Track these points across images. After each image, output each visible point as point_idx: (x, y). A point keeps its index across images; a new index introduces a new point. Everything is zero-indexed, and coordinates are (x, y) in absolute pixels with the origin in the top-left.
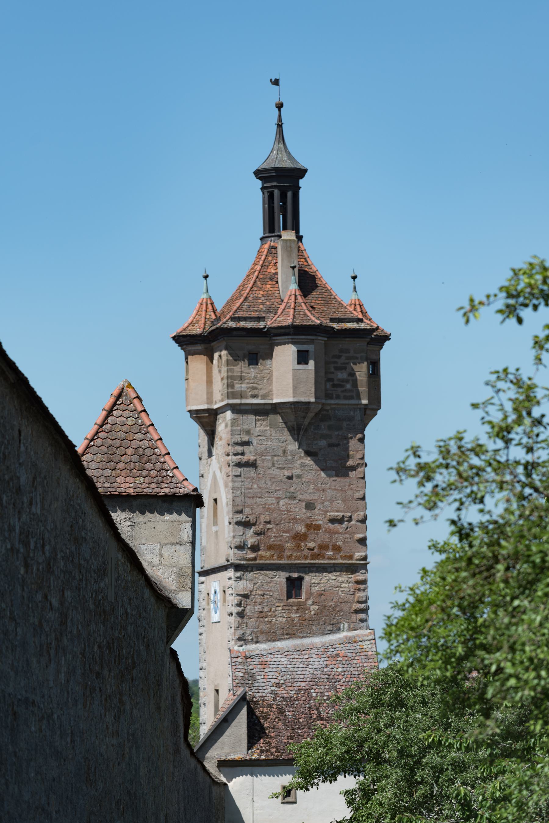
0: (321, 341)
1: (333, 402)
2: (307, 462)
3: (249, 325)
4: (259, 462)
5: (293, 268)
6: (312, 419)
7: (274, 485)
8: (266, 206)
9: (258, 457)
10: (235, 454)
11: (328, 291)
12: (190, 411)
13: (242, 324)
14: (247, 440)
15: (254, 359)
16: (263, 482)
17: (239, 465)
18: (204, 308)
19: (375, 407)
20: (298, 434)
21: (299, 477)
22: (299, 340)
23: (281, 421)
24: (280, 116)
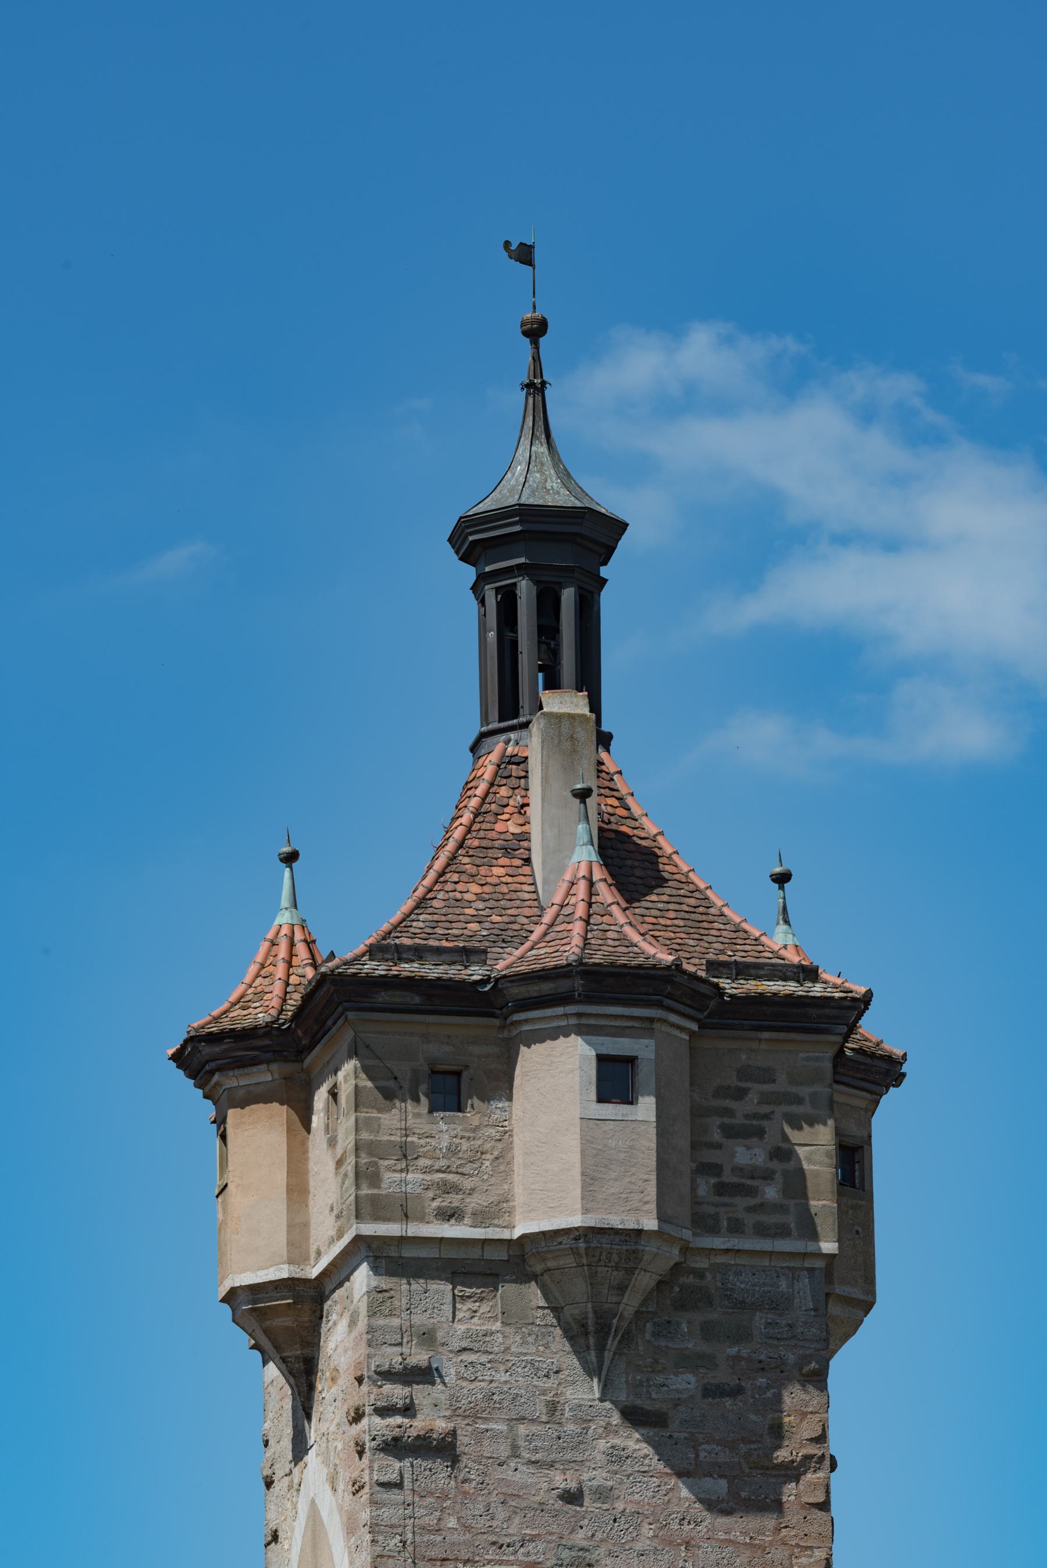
0: (677, 1033)
1: (718, 1242)
2: (632, 1445)
3: (432, 971)
4: (463, 1440)
5: (583, 795)
6: (645, 1302)
7: (517, 1520)
8: (492, 635)
9: (461, 1423)
10: (383, 1412)
11: (697, 895)
12: (231, 1297)
13: (408, 968)
14: (424, 1364)
15: (449, 1089)
16: (480, 1508)
17: (394, 1447)
18: (282, 952)
19: (857, 1293)
20: (601, 1349)
21: (603, 1494)
22: (603, 1022)
23: (542, 1303)
24: (536, 359)
